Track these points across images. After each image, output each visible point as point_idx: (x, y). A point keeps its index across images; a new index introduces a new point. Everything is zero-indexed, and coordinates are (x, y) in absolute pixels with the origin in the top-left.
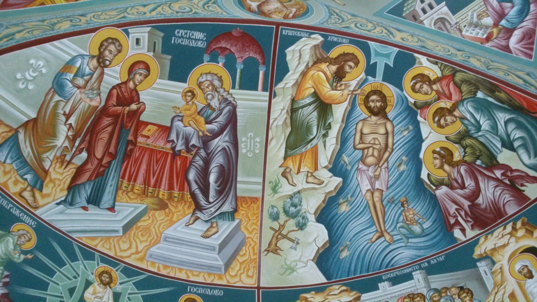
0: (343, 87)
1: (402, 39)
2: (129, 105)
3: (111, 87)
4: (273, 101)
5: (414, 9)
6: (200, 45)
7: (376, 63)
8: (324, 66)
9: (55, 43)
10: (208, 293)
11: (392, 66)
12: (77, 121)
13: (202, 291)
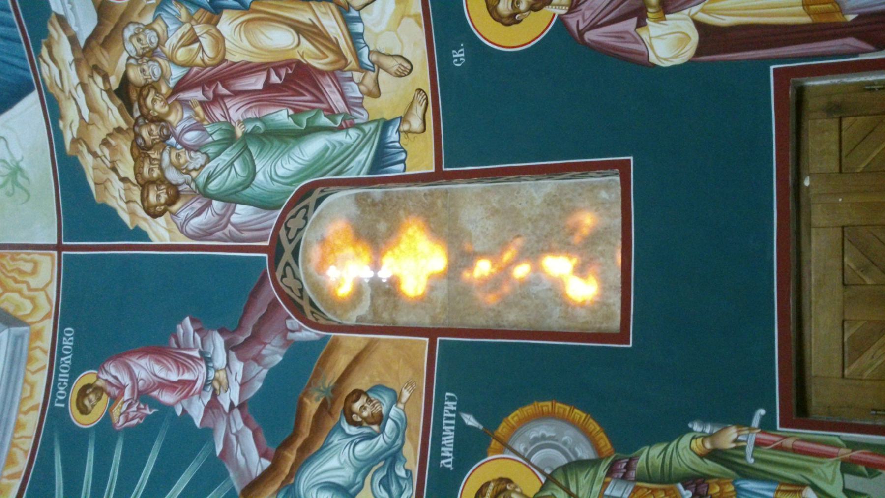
10: (69, 362)
13: (64, 374)
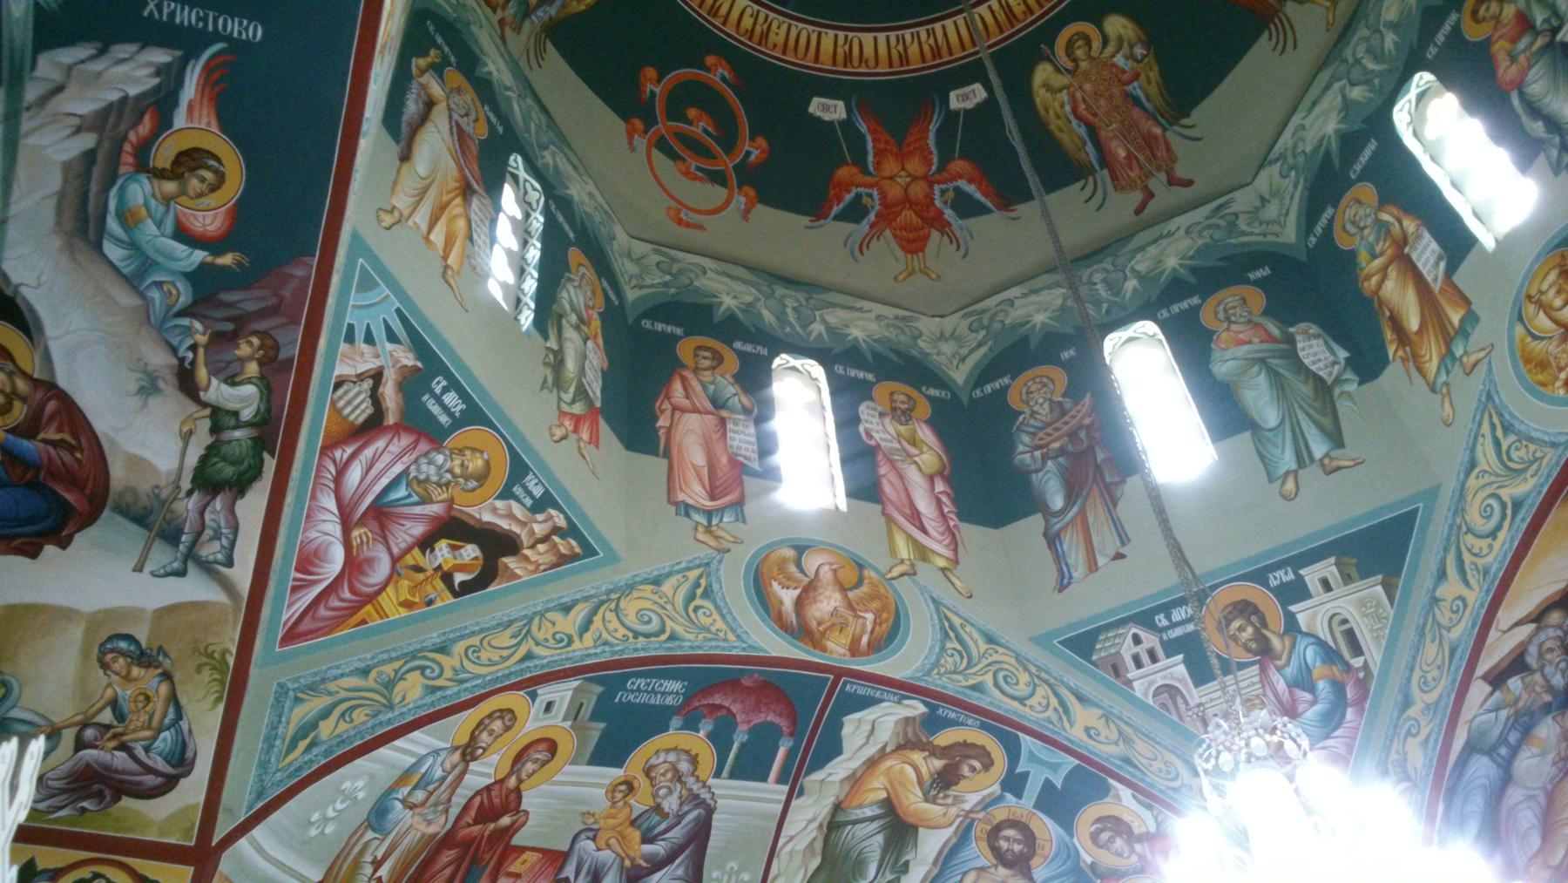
0: (950, 801)
1: (1087, 730)
2: (497, 817)
3: (472, 794)
4: (794, 803)
5: (1118, 653)
6: (669, 701)
7: (1026, 775)
8: (918, 757)
9: (398, 743)
11: (1059, 786)
12: (392, 872)
